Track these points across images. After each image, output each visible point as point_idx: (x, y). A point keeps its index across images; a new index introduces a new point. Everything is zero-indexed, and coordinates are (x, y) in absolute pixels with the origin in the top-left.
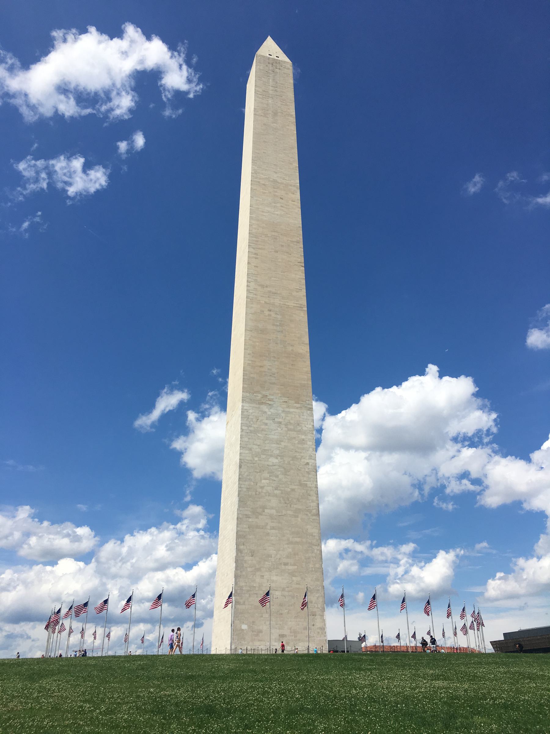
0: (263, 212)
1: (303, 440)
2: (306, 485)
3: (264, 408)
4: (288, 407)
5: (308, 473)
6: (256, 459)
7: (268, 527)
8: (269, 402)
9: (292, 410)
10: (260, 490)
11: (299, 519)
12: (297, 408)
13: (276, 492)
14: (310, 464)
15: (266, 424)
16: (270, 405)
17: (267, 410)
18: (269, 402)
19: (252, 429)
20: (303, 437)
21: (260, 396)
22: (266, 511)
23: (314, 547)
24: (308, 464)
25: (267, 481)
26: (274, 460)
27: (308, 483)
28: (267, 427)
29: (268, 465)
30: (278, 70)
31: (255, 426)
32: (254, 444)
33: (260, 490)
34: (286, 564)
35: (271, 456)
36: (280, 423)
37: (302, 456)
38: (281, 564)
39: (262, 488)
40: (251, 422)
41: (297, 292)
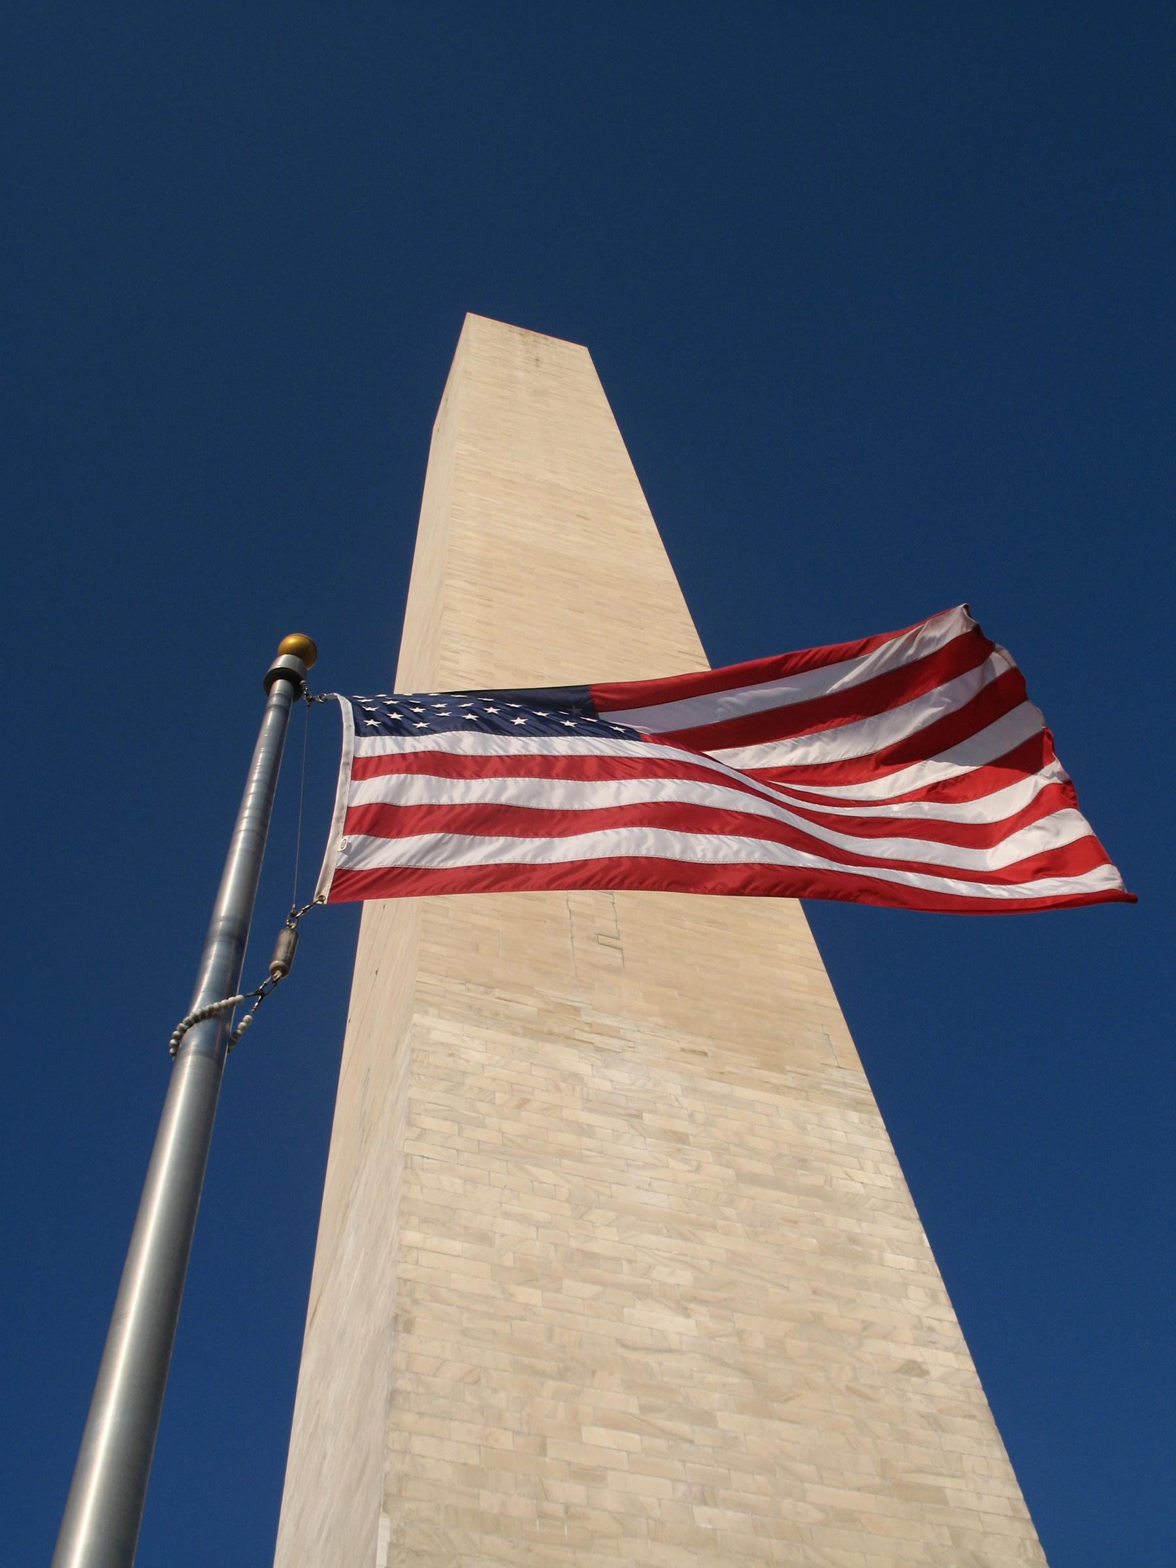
1: (853, 1239)
2: (938, 1496)
3: (569, 1059)
4: (721, 1076)
6: (530, 1295)
10: (575, 1492)
12: (777, 1089)
13: (704, 1516)
14: (935, 1372)
15: (587, 1131)
16: (599, 1049)
17: (584, 1068)
20: (848, 1224)
24: (914, 1369)
25: (633, 1440)
27: (947, 1483)
28: (587, 1142)
31: (508, 1126)
32: (508, 1215)
33: (575, 1492)
35: (642, 1293)
37: (867, 1325)
39: (590, 1476)
40: (483, 1107)
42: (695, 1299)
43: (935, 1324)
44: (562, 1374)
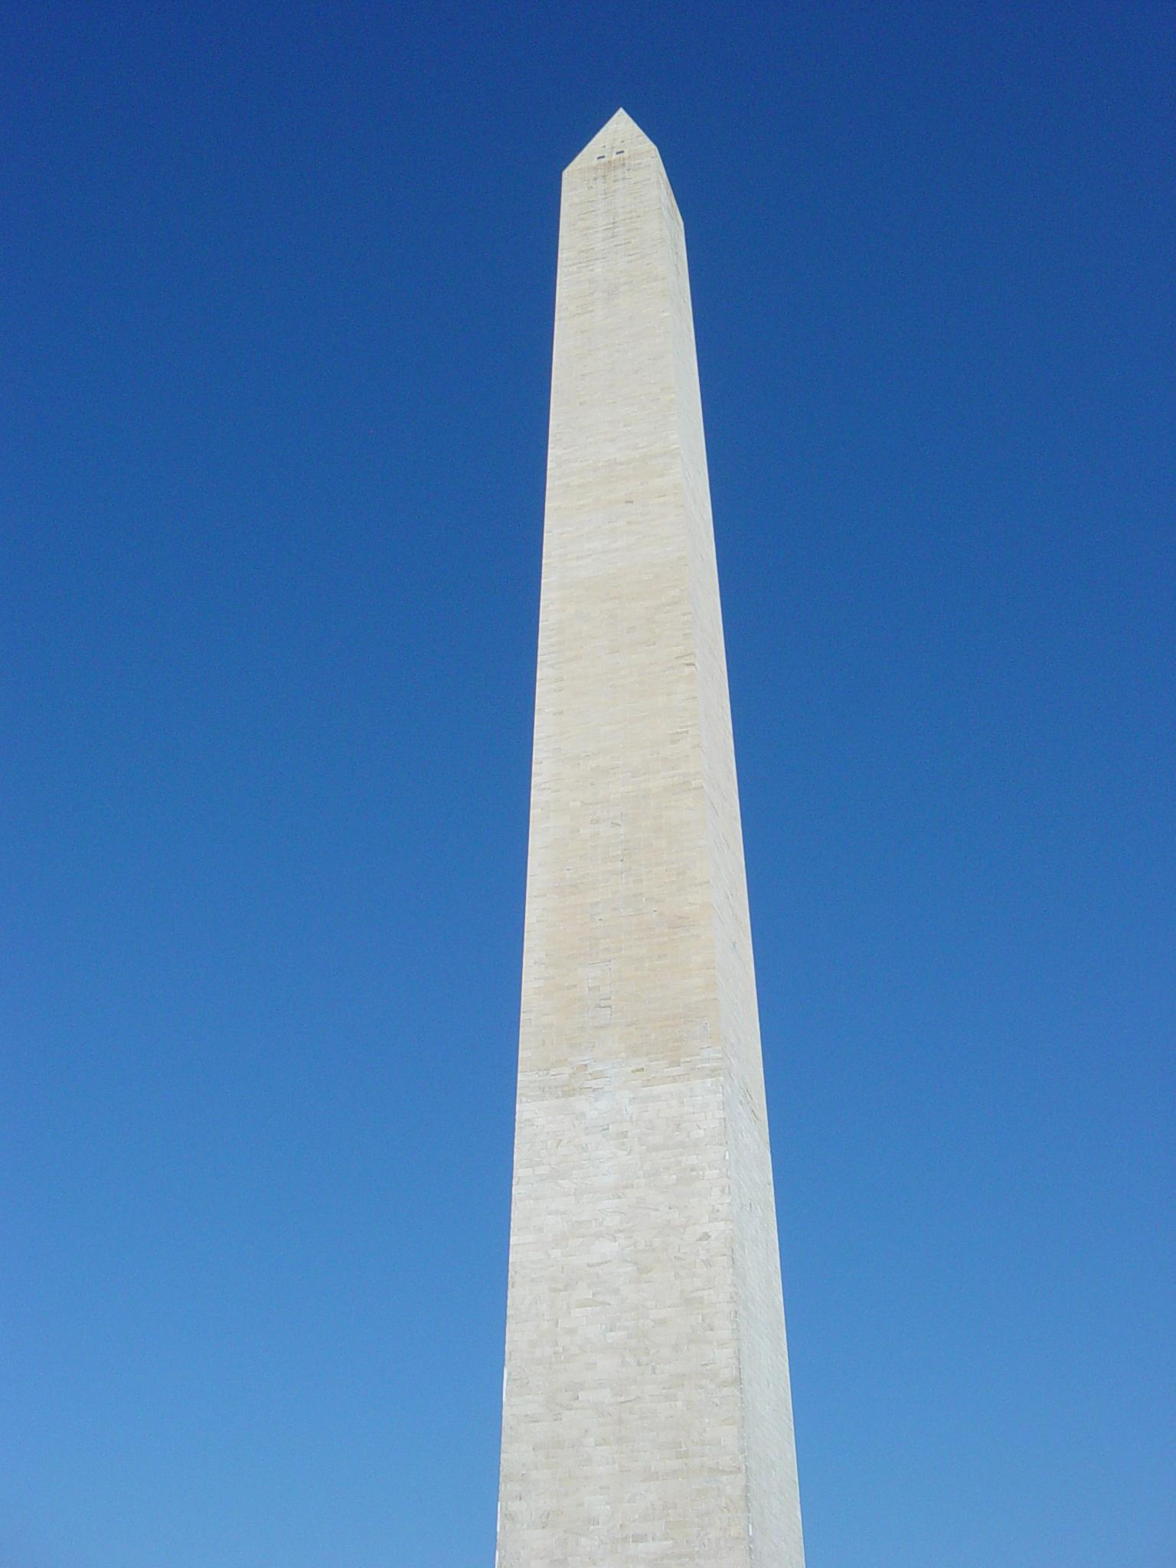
0: (578, 558)
5: (708, 1263)
6: (556, 1253)
7: (591, 1440)
8: (593, 1084)
9: (658, 1089)
11: (679, 1403)
18: (593, 1084)
19: (543, 1170)
21: (567, 1071)
22: (581, 1395)
23: (724, 1478)
24: (706, 1236)
26: (607, 1248)
29: (589, 1265)
30: (619, 185)
34: (638, 1538)
36: (624, 1135)
38: (625, 1539)
39: (571, 1332)
41: (673, 742)
42: (620, 1231)
43: (720, 1207)
44: (566, 1290)
